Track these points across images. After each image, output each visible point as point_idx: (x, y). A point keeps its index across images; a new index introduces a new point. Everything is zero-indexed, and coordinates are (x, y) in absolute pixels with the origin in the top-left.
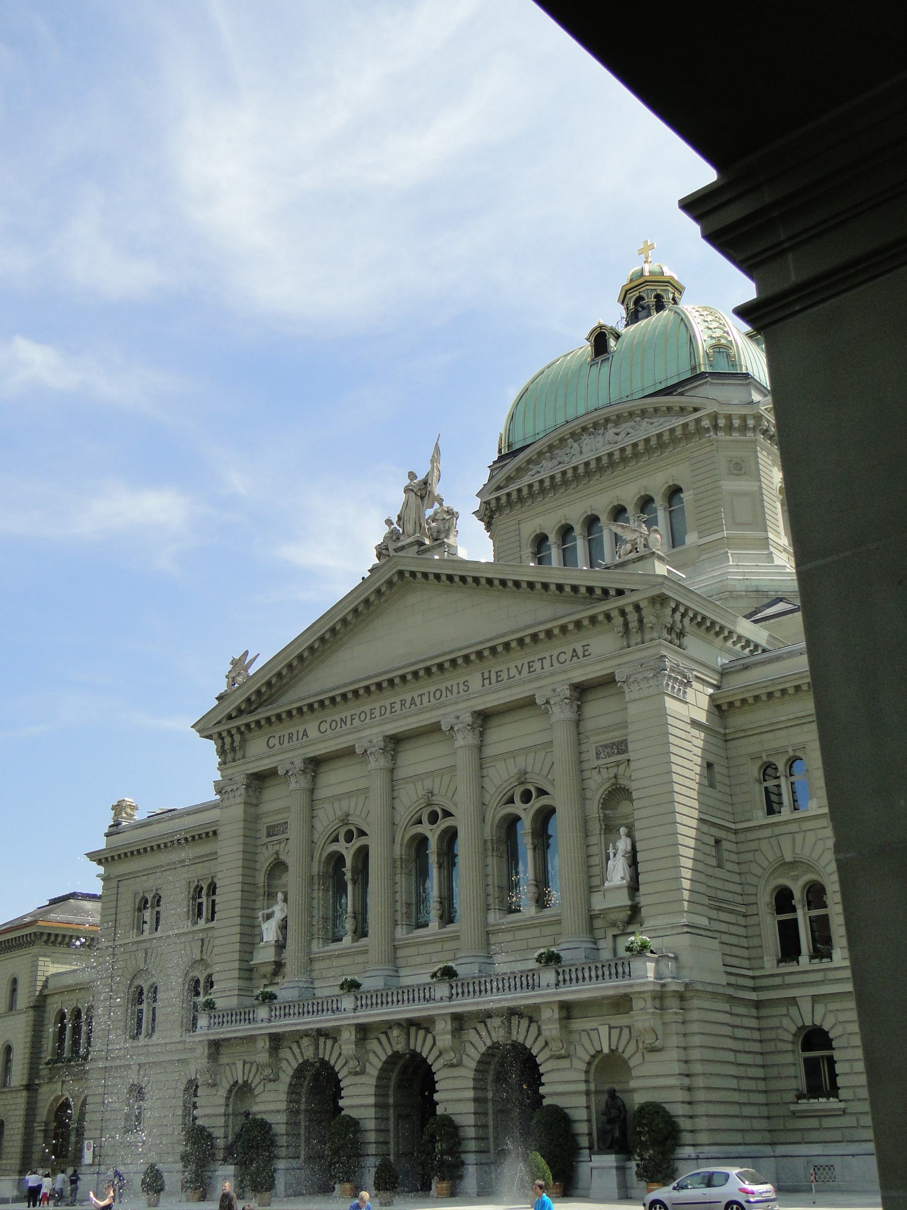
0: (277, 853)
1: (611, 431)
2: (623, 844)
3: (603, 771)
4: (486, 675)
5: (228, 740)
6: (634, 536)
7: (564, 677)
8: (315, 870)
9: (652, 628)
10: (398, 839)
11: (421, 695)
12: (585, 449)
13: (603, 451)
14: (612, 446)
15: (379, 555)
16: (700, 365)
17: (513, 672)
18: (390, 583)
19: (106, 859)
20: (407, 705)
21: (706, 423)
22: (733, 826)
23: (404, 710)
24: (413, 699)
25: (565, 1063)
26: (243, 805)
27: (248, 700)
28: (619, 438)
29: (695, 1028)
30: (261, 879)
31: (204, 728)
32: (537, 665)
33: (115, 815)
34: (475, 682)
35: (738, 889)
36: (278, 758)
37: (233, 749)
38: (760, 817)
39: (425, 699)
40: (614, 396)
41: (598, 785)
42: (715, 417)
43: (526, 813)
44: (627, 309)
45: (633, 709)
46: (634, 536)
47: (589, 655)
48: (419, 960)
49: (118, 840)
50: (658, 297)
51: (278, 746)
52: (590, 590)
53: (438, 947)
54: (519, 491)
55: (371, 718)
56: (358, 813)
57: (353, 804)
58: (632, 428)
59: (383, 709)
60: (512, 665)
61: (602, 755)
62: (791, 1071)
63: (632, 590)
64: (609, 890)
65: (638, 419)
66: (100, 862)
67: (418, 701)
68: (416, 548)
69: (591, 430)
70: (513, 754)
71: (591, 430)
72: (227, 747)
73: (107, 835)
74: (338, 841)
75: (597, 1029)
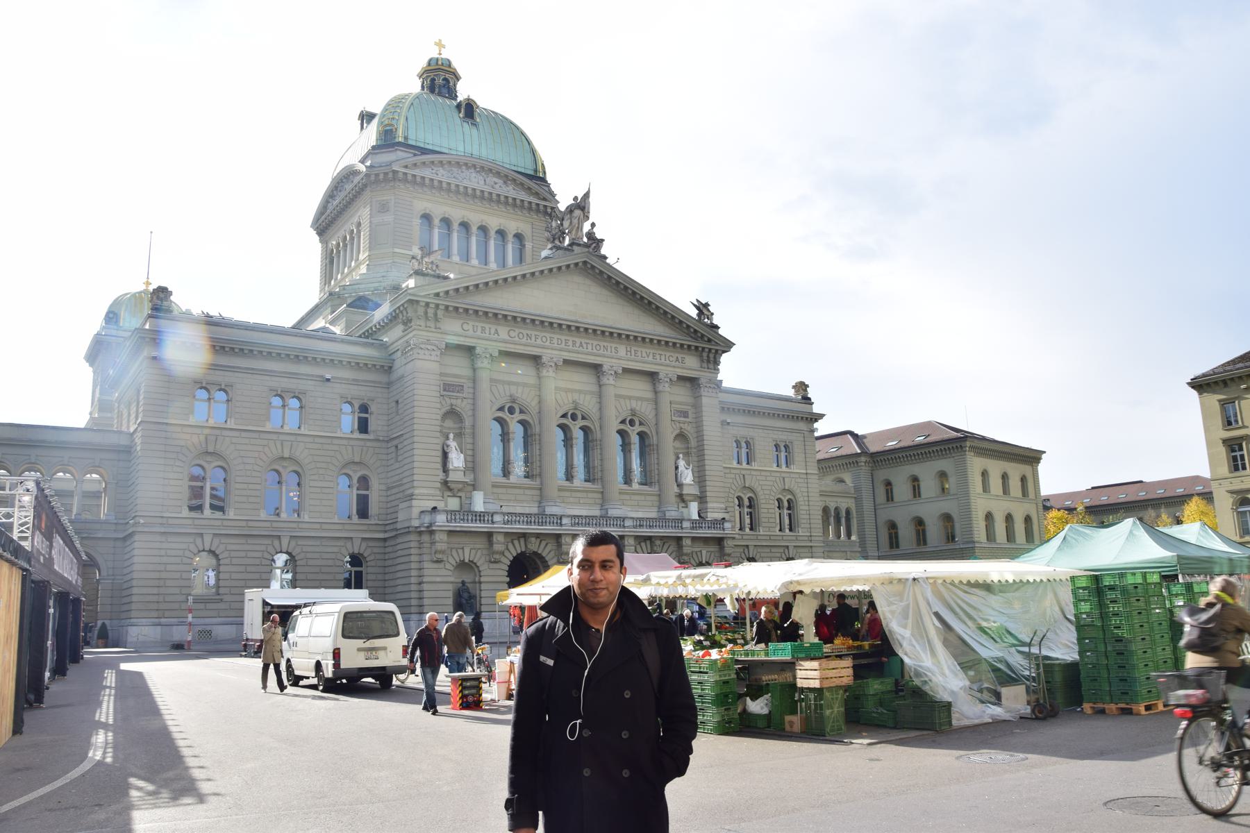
1: (492, 179)
3: (678, 424)
4: (629, 349)
5: (431, 312)
11: (587, 343)
12: (474, 180)
13: (487, 189)
16: (539, 172)
17: (644, 354)
18: (576, 264)
21: (549, 210)
23: (575, 348)
24: (581, 343)
28: (497, 186)
32: (658, 357)
34: (622, 350)
36: (475, 341)
39: (590, 347)
40: (484, 154)
45: (705, 400)
48: (571, 499)
51: (471, 333)
52: (696, 331)
53: (584, 495)
54: (423, 178)
57: (520, 391)
60: (644, 350)
61: (676, 415)
62: (370, 577)
63: (717, 343)
67: (585, 346)
70: (630, 398)
74: (504, 411)
75: (701, 551)
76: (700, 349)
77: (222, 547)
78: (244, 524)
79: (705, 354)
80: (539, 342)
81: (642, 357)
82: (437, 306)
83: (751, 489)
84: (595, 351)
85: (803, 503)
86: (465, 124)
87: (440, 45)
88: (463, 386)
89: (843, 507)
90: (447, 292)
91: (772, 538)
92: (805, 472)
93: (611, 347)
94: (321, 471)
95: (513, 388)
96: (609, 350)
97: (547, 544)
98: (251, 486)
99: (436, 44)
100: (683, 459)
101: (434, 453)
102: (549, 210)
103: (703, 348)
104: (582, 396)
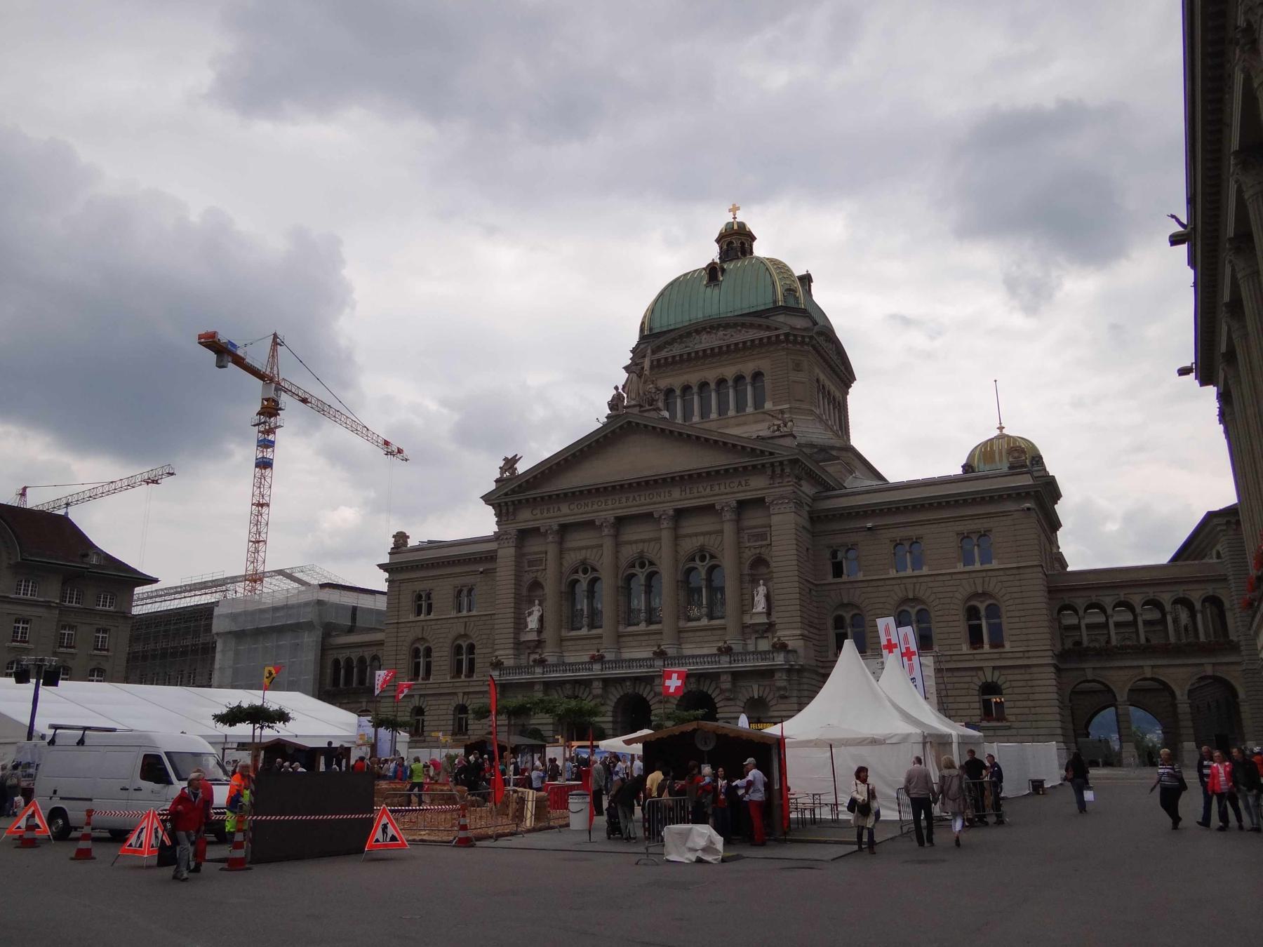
0: (536, 577)
1: (721, 333)
2: (762, 590)
3: (752, 549)
4: (683, 487)
6: (779, 422)
7: (733, 496)
8: (563, 589)
9: (789, 476)
10: (620, 576)
12: (703, 340)
13: (716, 343)
14: (722, 342)
15: (611, 409)
17: (701, 489)
19: (392, 569)
20: (631, 500)
22: (815, 582)
24: (634, 497)
25: (731, 703)
26: (514, 548)
27: (520, 486)
28: (728, 336)
29: (805, 687)
30: (524, 592)
31: (487, 499)
32: (716, 487)
33: (395, 541)
34: (676, 493)
35: (816, 615)
37: (507, 513)
38: (830, 579)
39: (643, 498)
41: (749, 555)
42: (787, 335)
43: (702, 568)
44: (721, 248)
45: (775, 520)
46: (779, 422)
47: (749, 485)
49: (400, 558)
50: (742, 244)
51: (539, 516)
53: (646, 637)
55: (605, 505)
56: (592, 558)
58: (735, 332)
59: (614, 501)
63: (778, 454)
64: (754, 614)
65: (739, 328)
66: (386, 570)
67: (638, 499)
68: (638, 408)
69: (709, 330)
70: (696, 535)
71: (709, 330)
72: (504, 511)
73: (389, 553)
74: (577, 573)
76: (759, 467)
77: (469, 702)
78: (437, 686)
79: (769, 472)
80: (595, 507)
81: (698, 492)
82: (506, 503)
83: (916, 600)
84: (648, 500)
85: (1013, 608)
86: (708, 289)
87: (734, 209)
88: (542, 560)
89: (1196, 595)
90: (513, 491)
91: (954, 658)
92: (1014, 565)
93: (665, 492)
94: (485, 641)
95: (584, 552)
96: (662, 495)
97: (585, 689)
98: (443, 659)
99: (730, 211)
100: (764, 585)
101: (509, 620)
102: (791, 338)
103: (763, 465)
104: (646, 544)
